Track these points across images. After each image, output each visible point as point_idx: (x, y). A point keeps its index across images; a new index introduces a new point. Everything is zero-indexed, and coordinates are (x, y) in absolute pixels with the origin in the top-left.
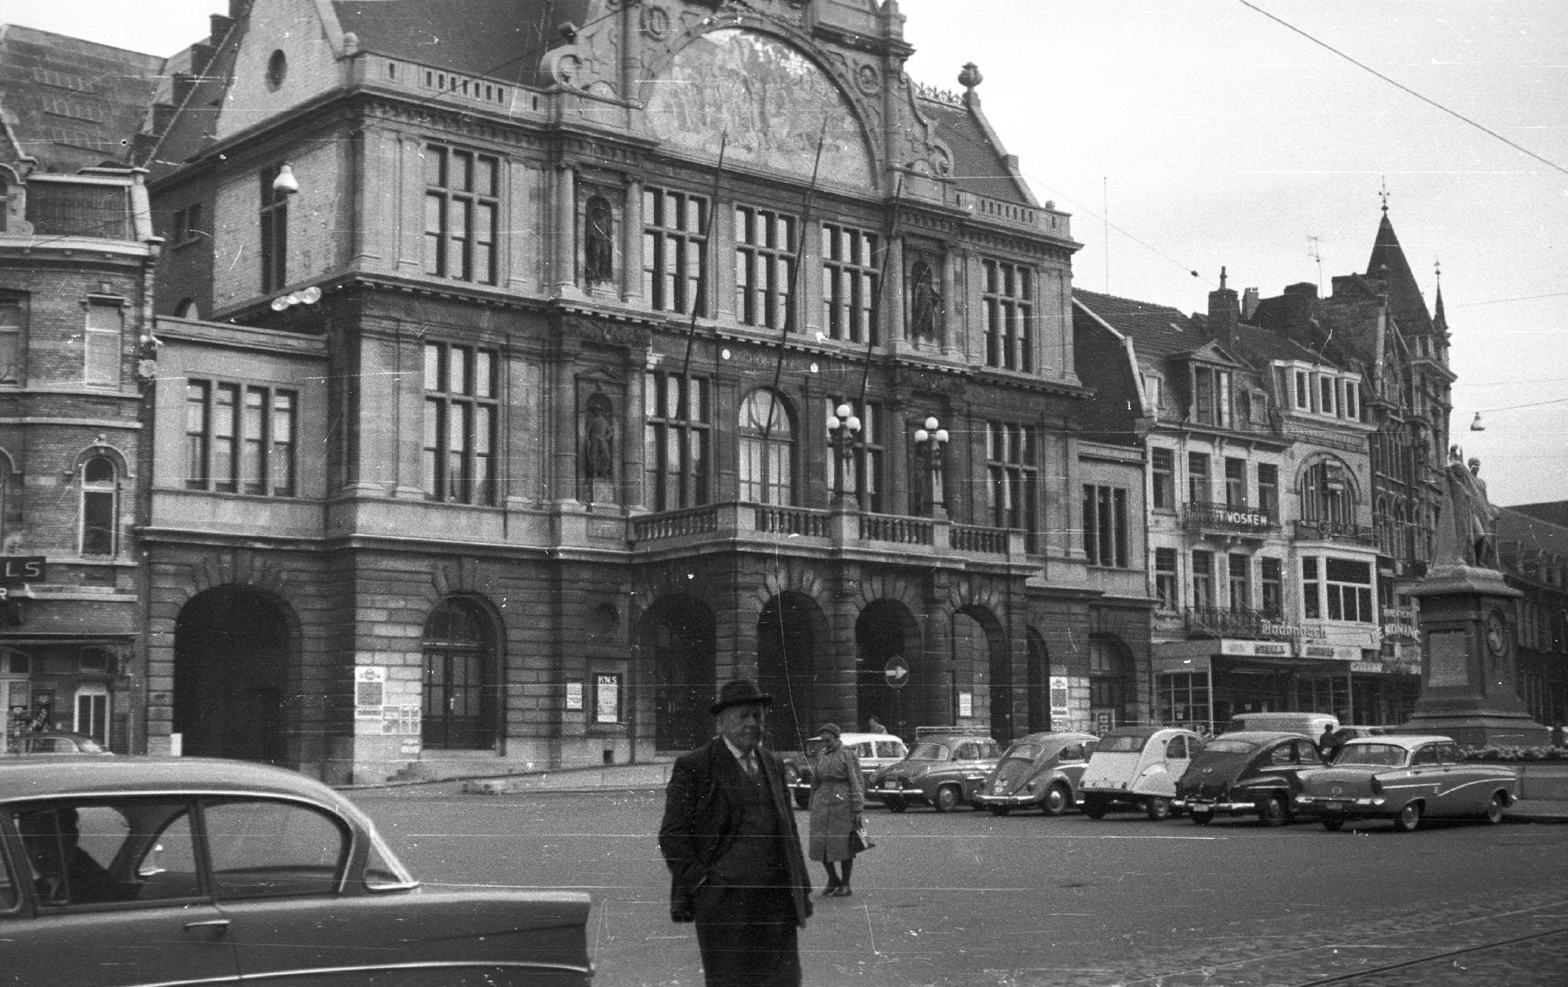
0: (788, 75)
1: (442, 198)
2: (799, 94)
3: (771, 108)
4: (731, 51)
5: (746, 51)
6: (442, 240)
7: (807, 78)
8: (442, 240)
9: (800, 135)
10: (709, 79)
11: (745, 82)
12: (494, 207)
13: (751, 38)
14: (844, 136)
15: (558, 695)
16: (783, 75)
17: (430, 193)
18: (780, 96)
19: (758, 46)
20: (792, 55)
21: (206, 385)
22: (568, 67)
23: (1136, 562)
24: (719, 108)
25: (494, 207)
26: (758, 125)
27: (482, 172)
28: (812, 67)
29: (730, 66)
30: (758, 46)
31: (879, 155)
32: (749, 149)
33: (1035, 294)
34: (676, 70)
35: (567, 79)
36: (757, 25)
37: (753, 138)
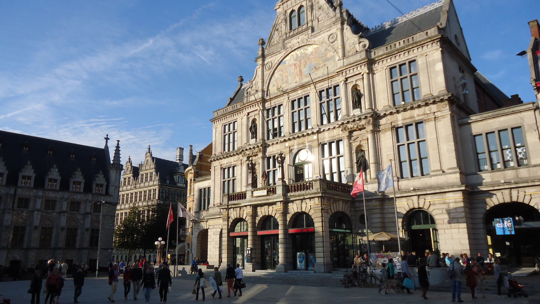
2: (311, 57)
11: (295, 65)
13: (296, 51)
24: (287, 77)
26: (299, 73)
28: (315, 46)
30: (298, 52)
32: (296, 82)
36: (296, 47)
37: (297, 79)
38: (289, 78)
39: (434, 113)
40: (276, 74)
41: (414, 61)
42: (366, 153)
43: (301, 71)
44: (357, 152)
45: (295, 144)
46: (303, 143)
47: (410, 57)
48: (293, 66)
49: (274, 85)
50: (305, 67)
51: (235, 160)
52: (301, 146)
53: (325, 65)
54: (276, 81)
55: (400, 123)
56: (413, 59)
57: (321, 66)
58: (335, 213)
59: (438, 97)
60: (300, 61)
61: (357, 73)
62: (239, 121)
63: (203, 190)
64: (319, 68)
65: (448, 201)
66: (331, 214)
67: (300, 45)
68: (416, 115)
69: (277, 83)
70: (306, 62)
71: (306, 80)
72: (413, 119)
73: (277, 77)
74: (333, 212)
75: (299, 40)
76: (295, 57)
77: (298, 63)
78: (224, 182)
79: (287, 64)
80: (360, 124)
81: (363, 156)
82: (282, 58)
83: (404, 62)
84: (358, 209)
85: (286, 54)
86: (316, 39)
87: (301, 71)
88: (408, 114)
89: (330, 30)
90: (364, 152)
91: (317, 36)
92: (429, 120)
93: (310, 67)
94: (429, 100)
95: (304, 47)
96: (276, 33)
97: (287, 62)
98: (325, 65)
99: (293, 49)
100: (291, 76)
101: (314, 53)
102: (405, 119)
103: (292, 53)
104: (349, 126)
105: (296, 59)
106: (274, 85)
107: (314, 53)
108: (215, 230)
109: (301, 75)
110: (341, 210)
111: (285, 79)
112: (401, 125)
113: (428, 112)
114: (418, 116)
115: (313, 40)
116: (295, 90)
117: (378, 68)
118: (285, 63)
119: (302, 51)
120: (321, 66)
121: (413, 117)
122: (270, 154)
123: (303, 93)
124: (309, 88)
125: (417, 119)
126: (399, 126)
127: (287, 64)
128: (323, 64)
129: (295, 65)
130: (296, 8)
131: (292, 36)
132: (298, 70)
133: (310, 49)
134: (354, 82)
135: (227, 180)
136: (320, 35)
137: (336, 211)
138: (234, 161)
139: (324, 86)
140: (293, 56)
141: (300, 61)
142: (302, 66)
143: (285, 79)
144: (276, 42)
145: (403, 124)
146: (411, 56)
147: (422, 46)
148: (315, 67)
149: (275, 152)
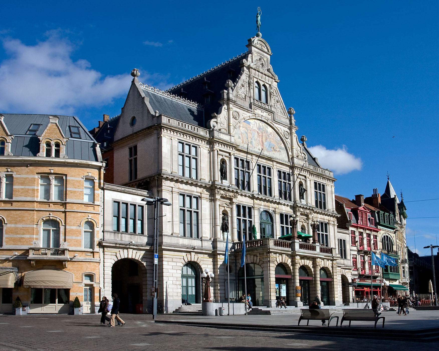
1: (183, 156)
3: (264, 139)
5: (258, 125)
6: (183, 166)
7: (272, 133)
8: (183, 166)
10: (249, 131)
11: (258, 132)
12: (196, 159)
15: (287, 293)
16: (267, 132)
17: (179, 154)
18: (266, 137)
19: (261, 124)
20: (269, 127)
21: (119, 203)
22: (215, 124)
23: (348, 257)
24: (252, 139)
25: (196, 159)
27: (193, 149)
28: (274, 131)
30: (261, 124)
31: (290, 154)
33: (326, 191)
34: (241, 128)
35: (215, 127)
43: (262, 141)
46: (268, 206)
48: (256, 133)
52: (266, 208)
64: (276, 151)
73: (242, 131)
77: (261, 134)
86: (277, 125)
87: (262, 141)
102: (321, 219)
107: (272, 135)
111: (250, 139)
122: (240, 202)
123: (267, 164)
124: (271, 163)
128: (278, 149)
141: (262, 133)
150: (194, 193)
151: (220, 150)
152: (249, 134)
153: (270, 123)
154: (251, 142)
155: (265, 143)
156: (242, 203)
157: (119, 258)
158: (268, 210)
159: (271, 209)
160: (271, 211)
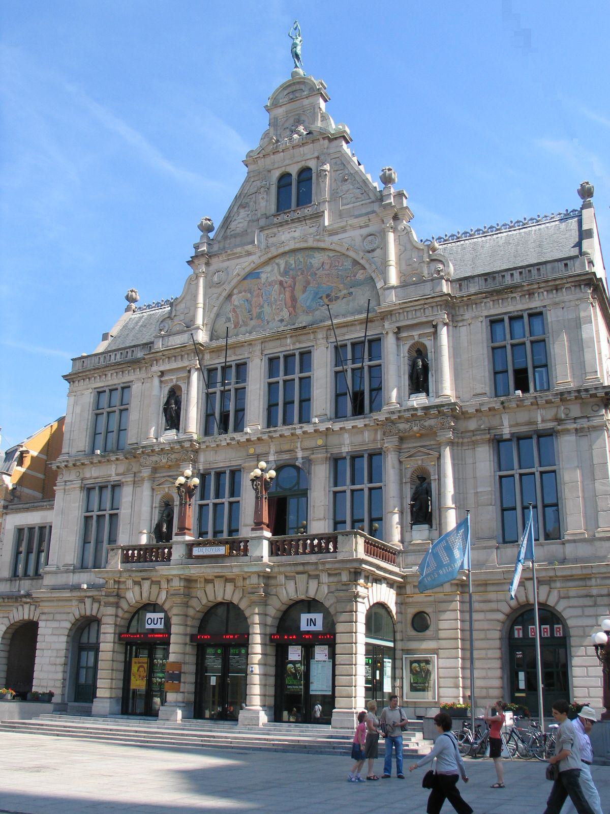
0: (312, 266)
2: (319, 273)
4: (272, 270)
9: (321, 298)
10: (255, 294)
11: (281, 283)
14: (356, 284)
20: (317, 255)
24: (262, 307)
26: (289, 304)
28: (331, 254)
29: (270, 280)
32: (282, 321)
34: (234, 297)
36: (287, 249)
37: (285, 314)
38: (267, 309)
39: (575, 419)
40: (236, 299)
41: (541, 314)
42: (434, 486)
43: (294, 299)
44: (412, 482)
45: (272, 451)
47: (532, 305)
48: (277, 287)
49: (229, 320)
50: (304, 292)
51: (121, 470)
53: (351, 294)
54: (234, 311)
55: (506, 432)
56: (538, 310)
57: (341, 294)
58: (374, 604)
59: (587, 390)
60: (294, 278)
61: (424, 319)
62: (136, 388)
63: (26, 531)
64: (337, 298)
65: (594, 591)
66: (368, 607)
67: (298, 246)
68: (539, 419)
69: (237, 317)
70: (308, 283)
71: (303, 320)
72: (533, 428)
73: (235, 303)
74: (371, 604)
75: (297, 234)
76: (282, 267)
78: (87, 519)
79: (263, 280)
80: (427, 424)
81: (428, 492)
82: (253, 266)
83: (520, 313)
84: (411, 600)
85: (263, 259)
86: (336, 238)
87: (294, 299)
88: (523, 417)
89: (367, 226)
90: (429, 484)
91: (337, 233)
92: (567, 431)
93: (317, 293)
94: (569, 392)
95: (307, 252)
96: (243, 213)
97: (263, 276)
98: (351, 294)
99: (281, 250)
100: (270, 304)
101: (327, 267)
102: (517, 425)
103: (277, 261)
104: (402, 426)
105: (285, 273)
106: (229, 320)
107: (327, 267)
108: (55, 624)
109: (294, 307)
110: (382, 600)
111: (255, 311)
112: (508, 437)
113: (563, 416)
114: (543, 421)
115: (326, 239)
116: (279, 336)
117: (466, 317)
118: (258, 277)
119: (300, 256)
120: (341, 294)
121: (535, 423)
122: (208, 466)
123: (298, 346)
125: (541, 426)
126: (505, 437)
127: (263, 280)
128: (345, 292)
129: (281, 283)
130: (294, 170)
131: (281, 225)
132: (288, 294)
133: (317, 259)
134: (416, 338)
135: (95, 514)
136: (345, 231)
137: (375, 602)
138: (117, 475)
139: (347, 337)
140: (278, 264)
141: (294, 278)
142: (299, 287)
143: (255, 311)
144: (238, 231)
145: (512, 434)
146: (535, 303)
147: (557, 289)
148: (328, 296)
149: (221, 465)
150: (112, 479)
151: (163, 373)
152: (254, 299)
153: (315, 245)
154: (259, 316)
155: (301, 297)
156: (215, 466)
157: (12, 622)
158: (291, 462)
159: (300, 454)
160: (299, 463)
